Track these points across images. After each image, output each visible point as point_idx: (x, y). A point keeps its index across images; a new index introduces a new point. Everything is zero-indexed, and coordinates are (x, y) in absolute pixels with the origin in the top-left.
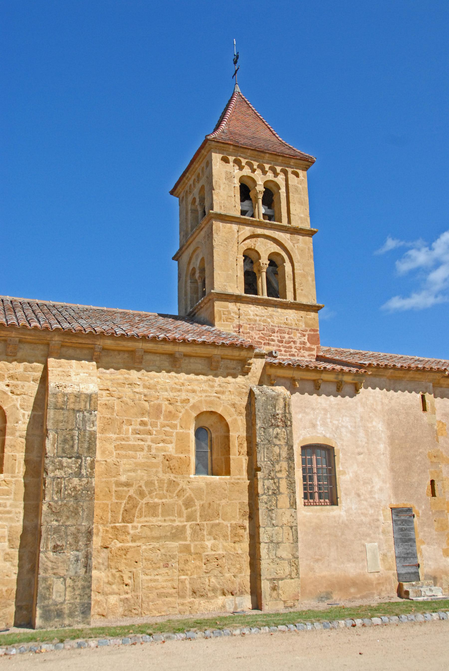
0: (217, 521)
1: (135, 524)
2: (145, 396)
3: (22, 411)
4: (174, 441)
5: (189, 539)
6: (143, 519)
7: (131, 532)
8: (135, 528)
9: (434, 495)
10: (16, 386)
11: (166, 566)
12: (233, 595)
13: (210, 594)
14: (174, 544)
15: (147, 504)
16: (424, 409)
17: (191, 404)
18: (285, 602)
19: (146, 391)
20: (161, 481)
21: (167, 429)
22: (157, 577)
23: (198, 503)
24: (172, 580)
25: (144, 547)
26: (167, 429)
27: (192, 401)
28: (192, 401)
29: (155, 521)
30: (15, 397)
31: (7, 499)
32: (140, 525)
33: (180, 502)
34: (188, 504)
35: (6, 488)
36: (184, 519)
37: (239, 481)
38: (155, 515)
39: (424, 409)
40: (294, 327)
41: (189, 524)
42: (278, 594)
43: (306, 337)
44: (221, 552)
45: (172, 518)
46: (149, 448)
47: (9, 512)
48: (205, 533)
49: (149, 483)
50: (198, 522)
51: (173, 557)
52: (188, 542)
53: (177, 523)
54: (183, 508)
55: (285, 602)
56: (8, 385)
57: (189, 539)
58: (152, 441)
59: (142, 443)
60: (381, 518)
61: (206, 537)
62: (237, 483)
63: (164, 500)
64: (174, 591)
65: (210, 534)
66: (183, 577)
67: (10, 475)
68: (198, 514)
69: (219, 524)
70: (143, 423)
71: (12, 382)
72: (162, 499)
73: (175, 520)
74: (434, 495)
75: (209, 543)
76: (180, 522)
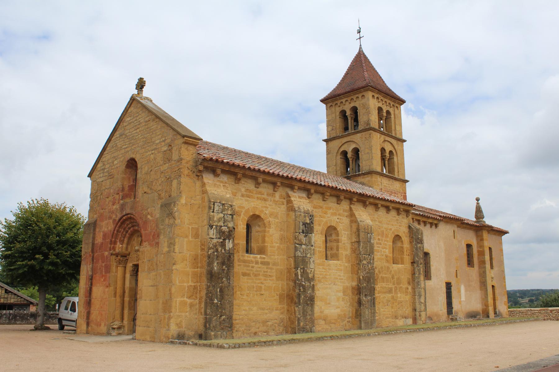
0: (401, 286)
1: (378, 286)
2: (379, 226)
3: (343, 232)
4: (388, 248)
5: (394, 293)
6: (381, 284)
7: (378, 289)
8: (378, 287)
9: (457, 277)
10: (340, 219)
11: (387, 305)
12: (405, 318)
13: (400, 318)
14: (390, 295)
15: (381, 277)
16: (454, 238)
17: (392, 231)
18: (423, 321)
19: (379, 224)
20: (385, 266)
21: (386, 242)
22: (385, 310)
23: (395, 277)
24: (389, 311)
25: (381, 296)
26: (386, 242)
27: (393, 229)
28: (393, 229)
29: (384, 285)
30: (340, 224)
31: (342, 273)
32: (380, 286)
33: (391, 277)
34: (393, 278)
35: (340, 268)
36: (392, 284)
37: (407, 268)
38: (384, 282)
39: (454, 238)
40: (398, 191)
41: (393, 286)
42: (421, 318)
43: (402, 197)
44: (402, 299)
45: (389, 284)
46: (381, 250)
47: (342, 279)
48: (398, 291)
49: (382, 268)
50: (396, 286)
51: (389, 301)
52: (393, 295)
53: (390, 286)
54: (392, 279)
55: (423, 321)
56: (338, 219)
57: (394, 293)
58: (382, 248)
59: (379, 249)
60: (443, 287)
61: (399, 293)
62: (406, 269)
63: (386, 276)
64: (390, 316)
65: (399, 291)
66: (392, 310)
67: (341, 262)
68: (396, 282)
69: (401, 287)
70: (379, 239)
71: (339, 217)
72: (385, 275)
73: (389, 285)
74: (457, 277)
75: (399, 295)
76: (391, 285)
